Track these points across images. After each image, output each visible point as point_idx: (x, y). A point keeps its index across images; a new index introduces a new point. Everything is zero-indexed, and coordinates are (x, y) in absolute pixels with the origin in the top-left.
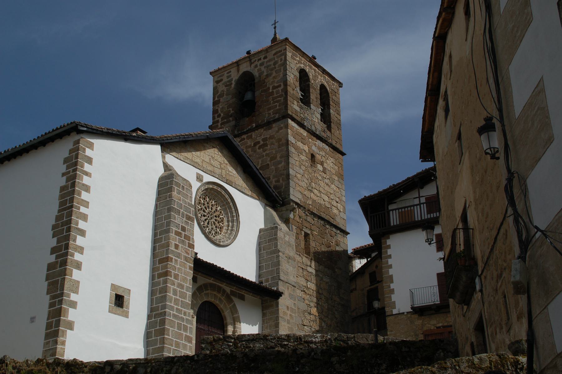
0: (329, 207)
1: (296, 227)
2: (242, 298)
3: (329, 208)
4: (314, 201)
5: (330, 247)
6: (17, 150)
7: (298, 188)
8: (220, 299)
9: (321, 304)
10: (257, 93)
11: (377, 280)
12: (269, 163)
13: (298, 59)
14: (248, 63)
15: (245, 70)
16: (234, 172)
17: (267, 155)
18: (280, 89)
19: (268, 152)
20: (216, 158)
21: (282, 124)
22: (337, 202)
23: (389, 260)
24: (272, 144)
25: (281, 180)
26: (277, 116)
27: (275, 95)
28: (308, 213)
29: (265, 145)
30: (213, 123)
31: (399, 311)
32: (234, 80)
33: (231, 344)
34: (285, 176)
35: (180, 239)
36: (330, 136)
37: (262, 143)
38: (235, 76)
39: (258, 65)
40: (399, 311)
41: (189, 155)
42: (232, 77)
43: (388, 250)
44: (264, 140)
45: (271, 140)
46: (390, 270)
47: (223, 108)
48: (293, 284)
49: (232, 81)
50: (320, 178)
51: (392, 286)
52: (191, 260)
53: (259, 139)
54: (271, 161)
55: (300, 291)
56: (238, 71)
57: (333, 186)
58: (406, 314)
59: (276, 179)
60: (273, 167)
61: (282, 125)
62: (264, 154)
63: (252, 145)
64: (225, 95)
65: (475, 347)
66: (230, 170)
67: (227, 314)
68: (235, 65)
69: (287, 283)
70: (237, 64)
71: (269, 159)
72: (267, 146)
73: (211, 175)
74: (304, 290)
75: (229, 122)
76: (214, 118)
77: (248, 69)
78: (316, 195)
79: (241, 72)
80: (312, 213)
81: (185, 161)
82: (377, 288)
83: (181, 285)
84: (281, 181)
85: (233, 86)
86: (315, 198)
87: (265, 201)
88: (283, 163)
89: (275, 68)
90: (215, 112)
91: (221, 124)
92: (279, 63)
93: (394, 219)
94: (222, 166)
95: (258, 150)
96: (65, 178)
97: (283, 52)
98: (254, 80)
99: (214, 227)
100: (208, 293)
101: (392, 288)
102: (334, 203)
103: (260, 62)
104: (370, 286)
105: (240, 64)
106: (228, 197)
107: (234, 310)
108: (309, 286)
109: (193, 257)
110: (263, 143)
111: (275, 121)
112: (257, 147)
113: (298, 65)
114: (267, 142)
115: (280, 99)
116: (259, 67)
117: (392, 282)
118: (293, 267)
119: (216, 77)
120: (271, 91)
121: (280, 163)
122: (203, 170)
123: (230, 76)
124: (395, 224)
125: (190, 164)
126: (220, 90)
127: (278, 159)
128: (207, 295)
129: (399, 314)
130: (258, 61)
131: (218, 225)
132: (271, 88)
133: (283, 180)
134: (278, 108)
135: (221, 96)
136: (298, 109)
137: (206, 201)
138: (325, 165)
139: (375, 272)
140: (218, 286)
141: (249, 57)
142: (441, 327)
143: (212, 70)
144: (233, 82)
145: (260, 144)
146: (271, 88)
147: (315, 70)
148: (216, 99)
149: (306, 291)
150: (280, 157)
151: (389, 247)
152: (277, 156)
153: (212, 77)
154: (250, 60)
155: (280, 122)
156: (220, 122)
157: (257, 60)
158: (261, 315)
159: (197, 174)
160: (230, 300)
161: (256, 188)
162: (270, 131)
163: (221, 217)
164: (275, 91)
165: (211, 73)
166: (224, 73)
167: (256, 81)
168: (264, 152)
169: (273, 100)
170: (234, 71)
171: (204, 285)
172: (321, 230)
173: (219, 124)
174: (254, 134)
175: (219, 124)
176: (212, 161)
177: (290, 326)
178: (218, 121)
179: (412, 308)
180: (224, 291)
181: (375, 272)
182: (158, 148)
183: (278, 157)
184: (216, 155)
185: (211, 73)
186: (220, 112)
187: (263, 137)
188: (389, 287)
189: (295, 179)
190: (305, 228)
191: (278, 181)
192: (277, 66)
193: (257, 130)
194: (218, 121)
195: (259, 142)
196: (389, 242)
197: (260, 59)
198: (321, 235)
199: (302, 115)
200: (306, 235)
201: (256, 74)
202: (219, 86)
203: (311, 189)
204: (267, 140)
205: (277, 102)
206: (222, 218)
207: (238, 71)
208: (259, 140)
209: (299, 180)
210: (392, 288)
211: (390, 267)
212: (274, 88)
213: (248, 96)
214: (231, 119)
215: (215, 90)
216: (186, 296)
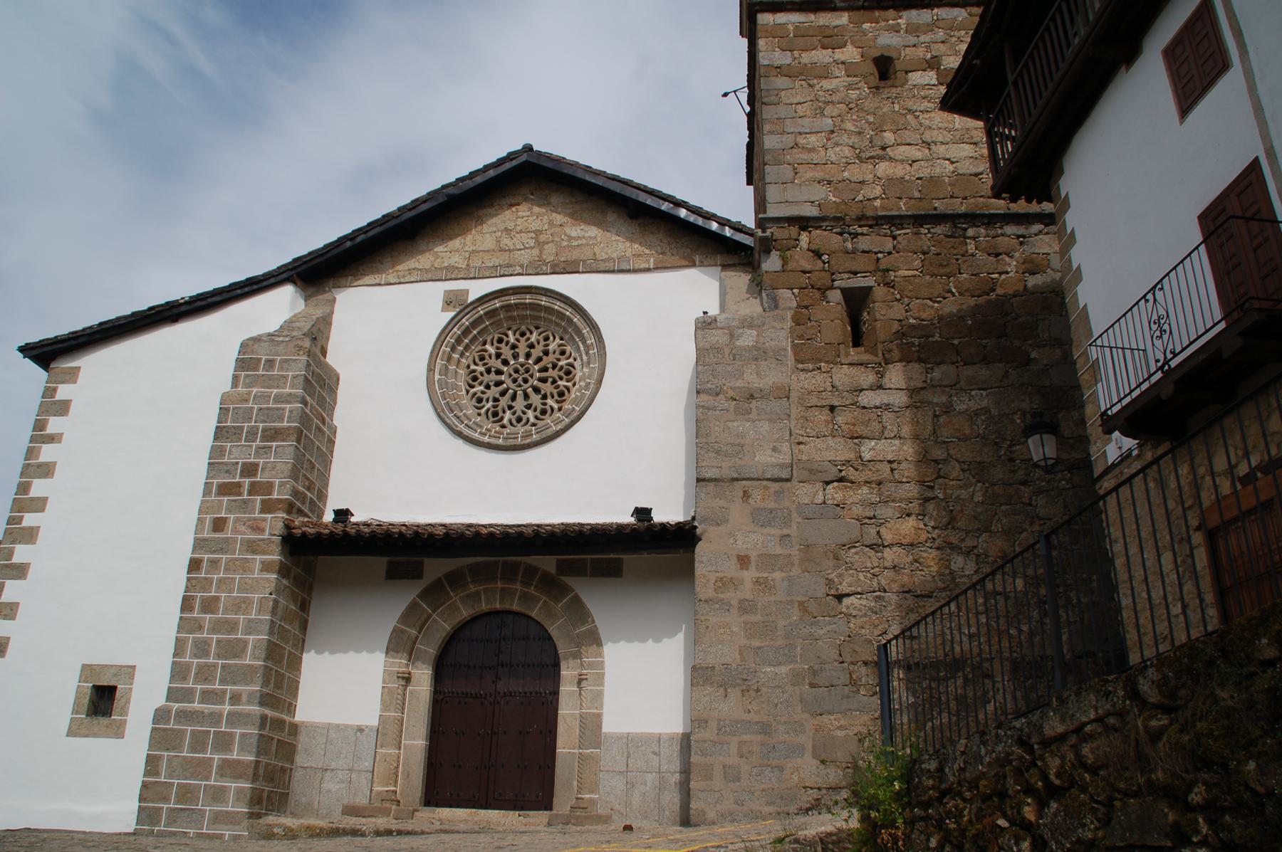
1: (796, 291)
7: (810, 175)
8: (526, 597)
9: (945, 494)
16: (593, 231)
28: (860, 226)
31: (1120, 448)
35: (233, 500)
40: (1120, 448)
41: (423, 261)
48: (776, 472)
52: (273, 542)
55: (819, 485)
66: (574, 234)
69: (737, 479)
73: (497, 277)
74: (843, 474)
81: (402, 280)
83: (227, 621)
87: (719, 259)
94: (542, 238)
106: (562, 305)
108: (867, 456)
109: (274, 535)
118: (770, 421)
122: (465, 276)
125: (421, 281)
128: (475, 597)
142: (1259, 475)
161: (683, 240)
172: (937, 254)
177: (756, 618)
180: (531, 571)
190: (846, 276)
198: (943, 271)
203: (881, 152)
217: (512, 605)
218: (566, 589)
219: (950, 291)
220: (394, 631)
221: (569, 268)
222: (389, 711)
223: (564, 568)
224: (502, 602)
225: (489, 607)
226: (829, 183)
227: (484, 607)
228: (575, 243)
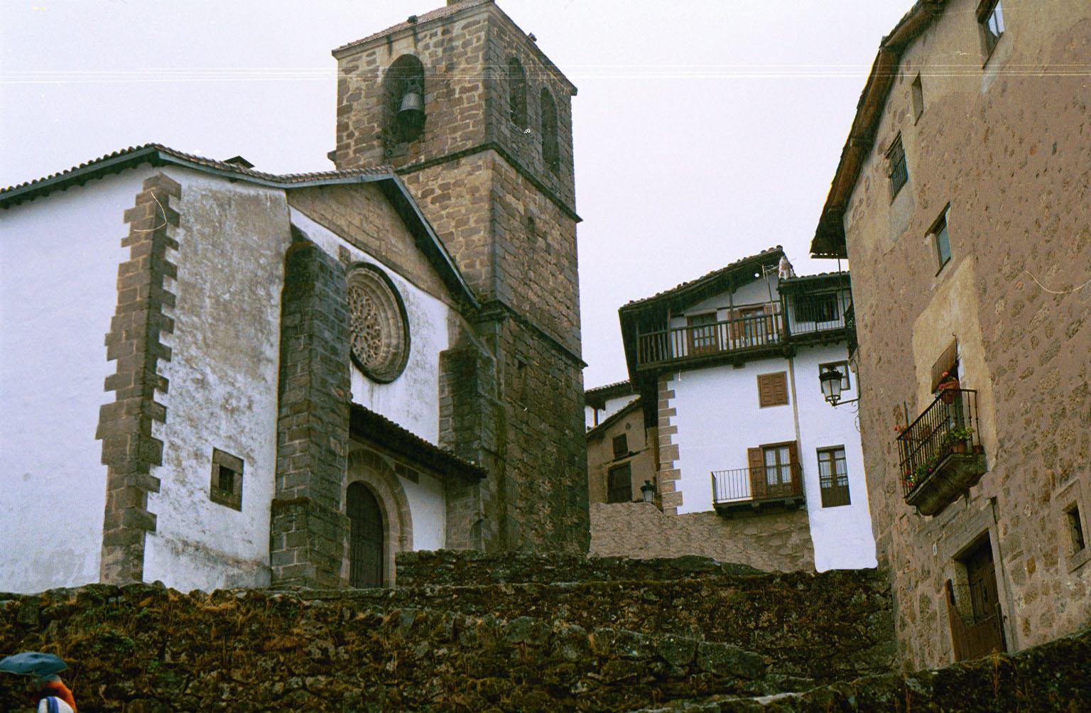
0: (556, 315)
2: (414, 478)
3: (555, 318)
4: (532, 304)
6: (26, 190)
10: (429, 98)
11: (629, 450)
12: (454, 230)
13: (507, 39)
14: (411, 39)
15: (405, 52)
16: (400, 246)
17: (449, 216)
18: (476, 94)
19: (452, 210)
20: (370, 219)
21: (480, 159)
22: (568, 308)
23: (672, 418)
24: (460, 196)
25: (478, 263)
26: (469, 145)
27: (466, 105)
29: (446, 197)
30: (339, 148)
32: (381, 68)
33: (452, 566)
34: (485, 258)
36: (558, 186)
37: (438, 192)
38: (383, 61)
39: (431, 45)
42: (377, 64)
43: (670, 400)
44: (441, 187)
45: (458, 189)
46: (673, 436)
47: (358, 121)
49: (378, 70)
50: (542, 262)
51: (677, 465)
53: (434, 185)
54: (456, 227)
56: (390, 51)
57: (561, 277)
59: (468, 261)
60: (461, 239)
61: (480, 163)
62: (444, 213)
63: (420, 196)
64: (363, 96)
65: (955, 588)
67: (390, 506)
68: (386, 41)
70: (389, 38)
71: (453, 224)
72: (449, 199)
75: (371, 148)
76: (339, 139)
77: (411, 51)
78: (536, 293)
79: (395, 57)
80: (534, 330)
82: (627, 465)
84: (478, 266)
85: (380, 80)
86: (535, 299)
88: (482, 232)
89: (466, 53)
90: (342, 127)
91: (355, 152)
92: (474, 45)
93: (680, 346)
94: (381, 235)
95: (431, 206)
96: (128, 249)
97: (482, 24)
98: (422, 71)
99: (365, 345)
101: (676, 468)
102: (563, 309)
103: (435, 39)
104: (614, 461)
105: (394, 41)
107: (400, 502)
110: (440, 192)
111: (465, 153)
112: (429, 199)
113: (508, 50)
114: (450, 191)
115: (475, 112)
116: (432, 49)
117: (677, 458)
119: (344, 61)
120: (457, 96)
121: (475, 231)
123: (374, 61)
124: (680, 355)
126: (352, 86)
127: (472, 224)
130: (430, 38)
131: (371, 342)
132: (457, 91)
133: (481, 263)
134: (471, 129)
135: (356, 96)
136: (507, 133)
137: (353, 297)
138: (549, 238)
139: (624, 436)
140: (376, 455)
141: (413, 28)
143: (336, 47)
144: (380, 73)
145: (435, 195)
146: (457, 91)
147: (534, 62)
148: (345, 103)
150: (476, 222)
151: (672, 394)
152: (468, 219)
153: (337, 61)
154: (415, 34)
155: (477, 155)
156: (353, 148)
157: (428, 36)
158: (444, 508)
159: (341, 247)
160: (393, 483)
162: (456, 171)
163: (377, 328)
164: (464, 96)
165: (334, 53)
166: (360, 55)
167: (427, 74)
168: (444, 209)
169: (461, 113)
170: (381, 52)
173: (351, 152)
174: (422, 176)
175: (351, 152)
176: (365, 225)
178: (348, 146)
179: (716, 505)
181: (624, 436)
183: (472, 221)
184: (371, 214)
185: (334, 53)
186: (351, 128)
187: (440, 181)
189: (504, 264)
191: (472, 265)
192: (469, 49)
193: (429, 167)
194: (348, 146)
195: (432, 191)
196: (671, 386)
197: (436, 34)
199: (514, 146)
201: (426, 60)
202: (351, 78)
204: (450, 188)
205: (469, 117)
207: (390, 51)
208: (432, 187)
209: (509, 265)
210: (676, 468)
211: (674, 430)
212: (464, 90)
213: (410, 102)
214: (375, 143)
215: (342, 85)
218: (398, 483)
221: (394, 268)
223: (400, 470)
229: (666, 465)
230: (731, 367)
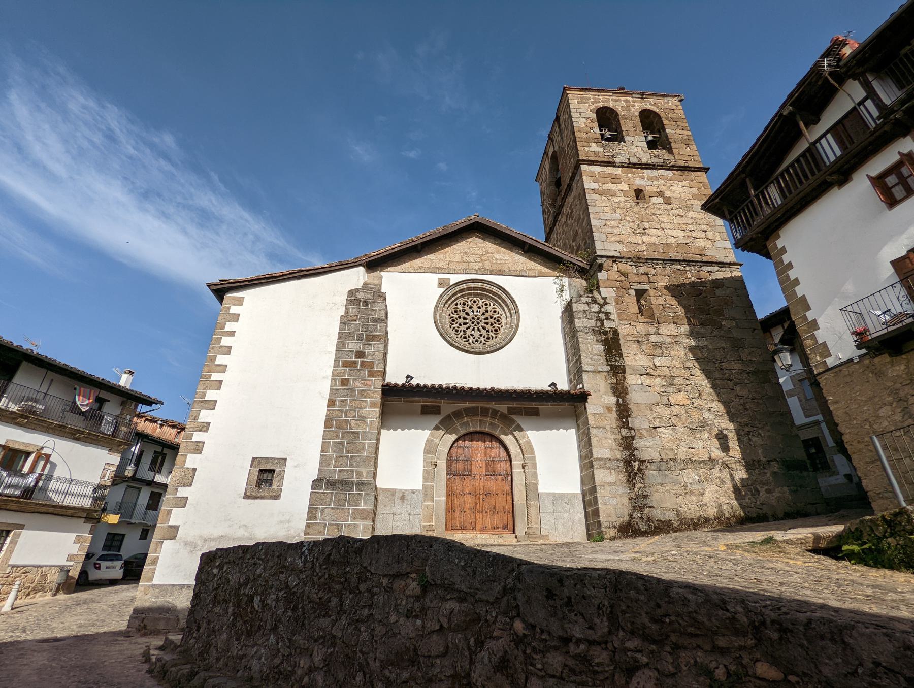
5: (701, 294)
7: (613, 239)
8: (491, 425)
37: (570, 211)
46: (797, 289)
58: (858, 360)
66: (498, 258)
74: (648, 371)
94: (483, 258)
100: (468, 422)
106: (496, 289)
108: (657, 364)
117: (808, 308)
128: (467, 424)
129: (842, 364)
149: (653, 372)
171: (454, 413)
180: (495, 413)
182: (361, 269)
188: (805, 318)
190: (636, 284)
196: (780, 244)
200: (640, 294)
203: (643, 231)
206: (498, 317)
216: (364, 447)
217: (485, 428)
218: (513, 422)
219: (682, 294)
220: (427, 440)
221: (500, 273)
222: (428, 482)
223: (512, 411)
224: (480, 427)
225: (474, 429)
226: (623, 243)
227: (471, 429)
228: (499, 262)
229: (801, 320)
230: (836, 188)
